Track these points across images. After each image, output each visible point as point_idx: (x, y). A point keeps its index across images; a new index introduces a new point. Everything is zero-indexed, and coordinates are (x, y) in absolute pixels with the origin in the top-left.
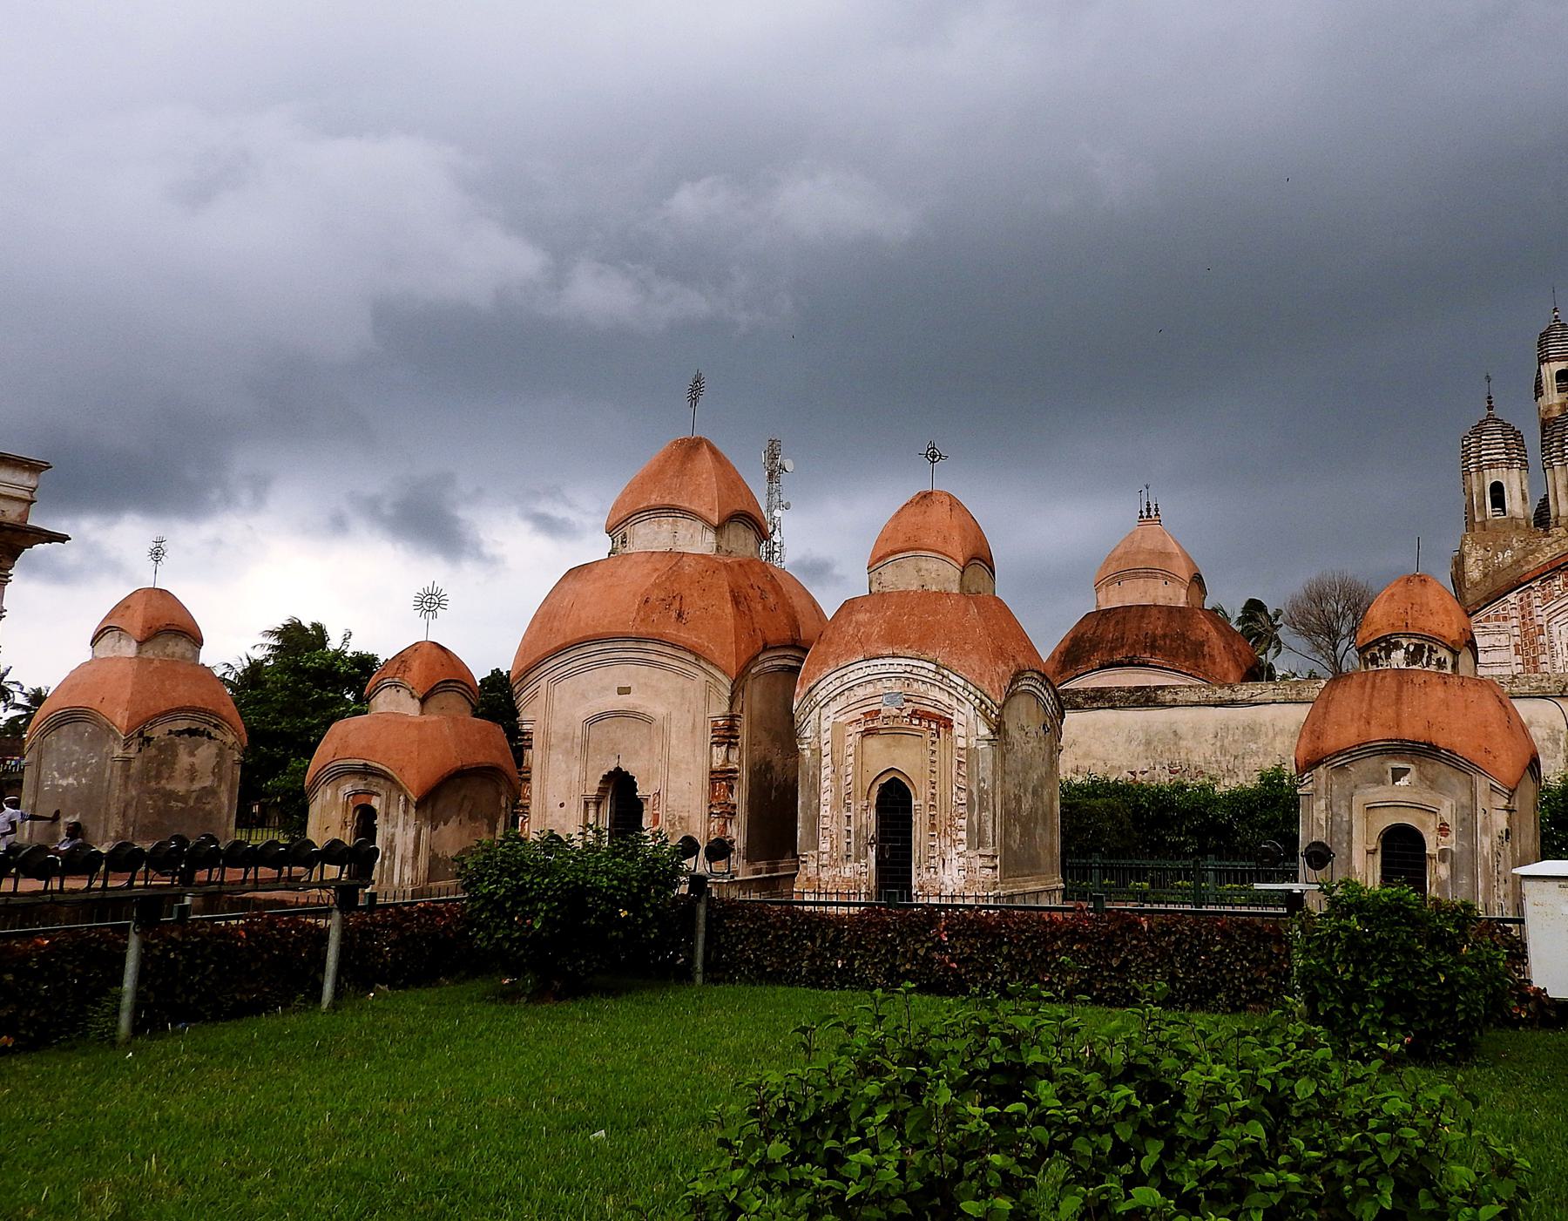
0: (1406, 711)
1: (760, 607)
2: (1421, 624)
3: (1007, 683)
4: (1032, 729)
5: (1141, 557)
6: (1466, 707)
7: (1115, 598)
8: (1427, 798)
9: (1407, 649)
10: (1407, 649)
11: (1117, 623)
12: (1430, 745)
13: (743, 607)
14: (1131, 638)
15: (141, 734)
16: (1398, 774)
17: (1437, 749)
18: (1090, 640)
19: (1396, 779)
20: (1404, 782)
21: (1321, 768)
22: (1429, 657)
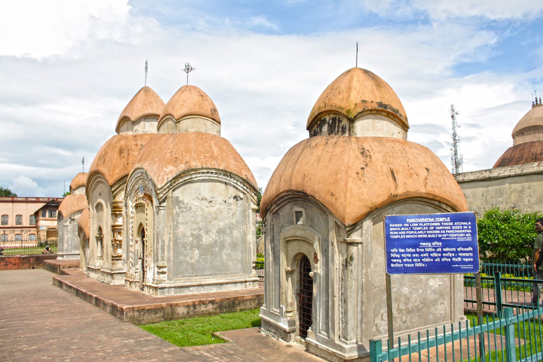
0: (297, 167)
1: (136, 153)
2: (332, 102)
3: (171, 177)
4: (220, 200)
5: (531, 121)
6: (330, 160)
7: (521, 140)
8: (307, 233)
9: (329, 123)
10: (329, 123)
11: (520, 150)
12: (304, 193)
13: (125, 154)
14: (525, 156)
15: (70, 218)
16: (298, 215)
17: (305, 194)
18: (509, 159)
19: (298, 220)
20: (300, 223)
21: (268, 214)
22: (338, 126)
